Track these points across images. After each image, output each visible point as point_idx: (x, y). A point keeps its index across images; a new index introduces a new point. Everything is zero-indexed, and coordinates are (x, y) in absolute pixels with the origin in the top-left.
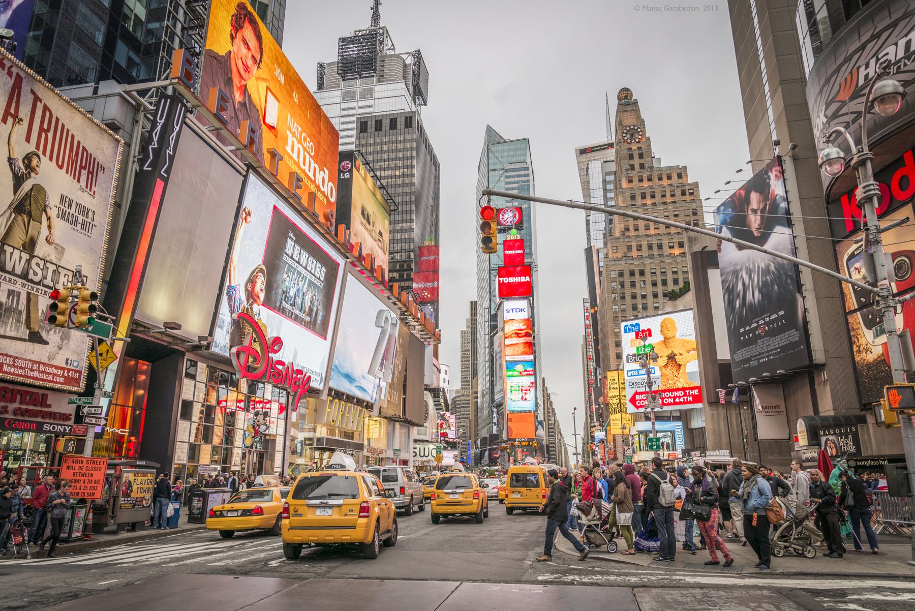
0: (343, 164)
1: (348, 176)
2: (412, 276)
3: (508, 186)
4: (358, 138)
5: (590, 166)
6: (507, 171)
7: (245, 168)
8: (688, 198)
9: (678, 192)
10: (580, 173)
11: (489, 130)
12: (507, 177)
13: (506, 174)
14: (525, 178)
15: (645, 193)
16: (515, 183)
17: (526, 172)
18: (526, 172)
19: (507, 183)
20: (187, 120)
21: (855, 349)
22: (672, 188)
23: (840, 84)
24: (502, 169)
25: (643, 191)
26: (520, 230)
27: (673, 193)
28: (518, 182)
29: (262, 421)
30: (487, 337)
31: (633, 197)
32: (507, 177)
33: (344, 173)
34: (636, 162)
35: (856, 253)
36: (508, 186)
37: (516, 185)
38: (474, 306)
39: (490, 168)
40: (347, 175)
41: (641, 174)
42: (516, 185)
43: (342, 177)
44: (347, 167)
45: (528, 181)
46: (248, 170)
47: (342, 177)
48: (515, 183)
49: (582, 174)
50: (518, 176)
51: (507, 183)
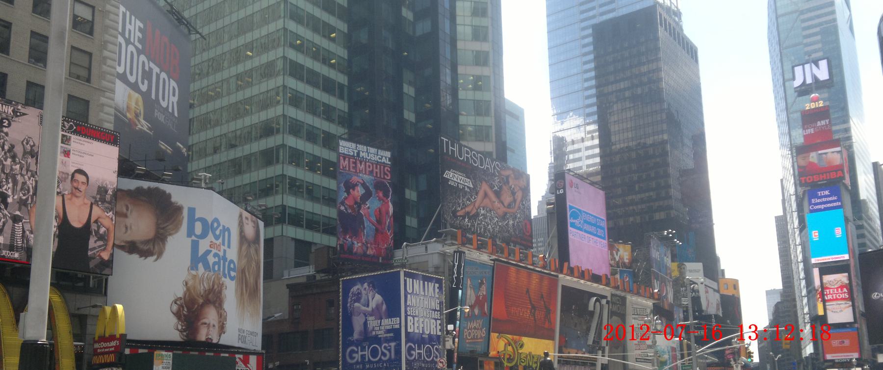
0: (558, 182)
6: (802, 12)
12: (803, 21)
13: (802, 17)
16: (815, 26)
17: (830, 9)
18: (830, 9)
19: (804, 29)
24: (795, 12)
28: (820, 24)
32: (803, 21)
33: (559, 190)
37: (818, 29)
39: (780, 12)
40: (561, 191)
42: (818, 29)
44: (561, 185)
45: (835, 20)
47: (558, 193)
48: (815, 26)
50: (819, 17)
51: (804, 29)
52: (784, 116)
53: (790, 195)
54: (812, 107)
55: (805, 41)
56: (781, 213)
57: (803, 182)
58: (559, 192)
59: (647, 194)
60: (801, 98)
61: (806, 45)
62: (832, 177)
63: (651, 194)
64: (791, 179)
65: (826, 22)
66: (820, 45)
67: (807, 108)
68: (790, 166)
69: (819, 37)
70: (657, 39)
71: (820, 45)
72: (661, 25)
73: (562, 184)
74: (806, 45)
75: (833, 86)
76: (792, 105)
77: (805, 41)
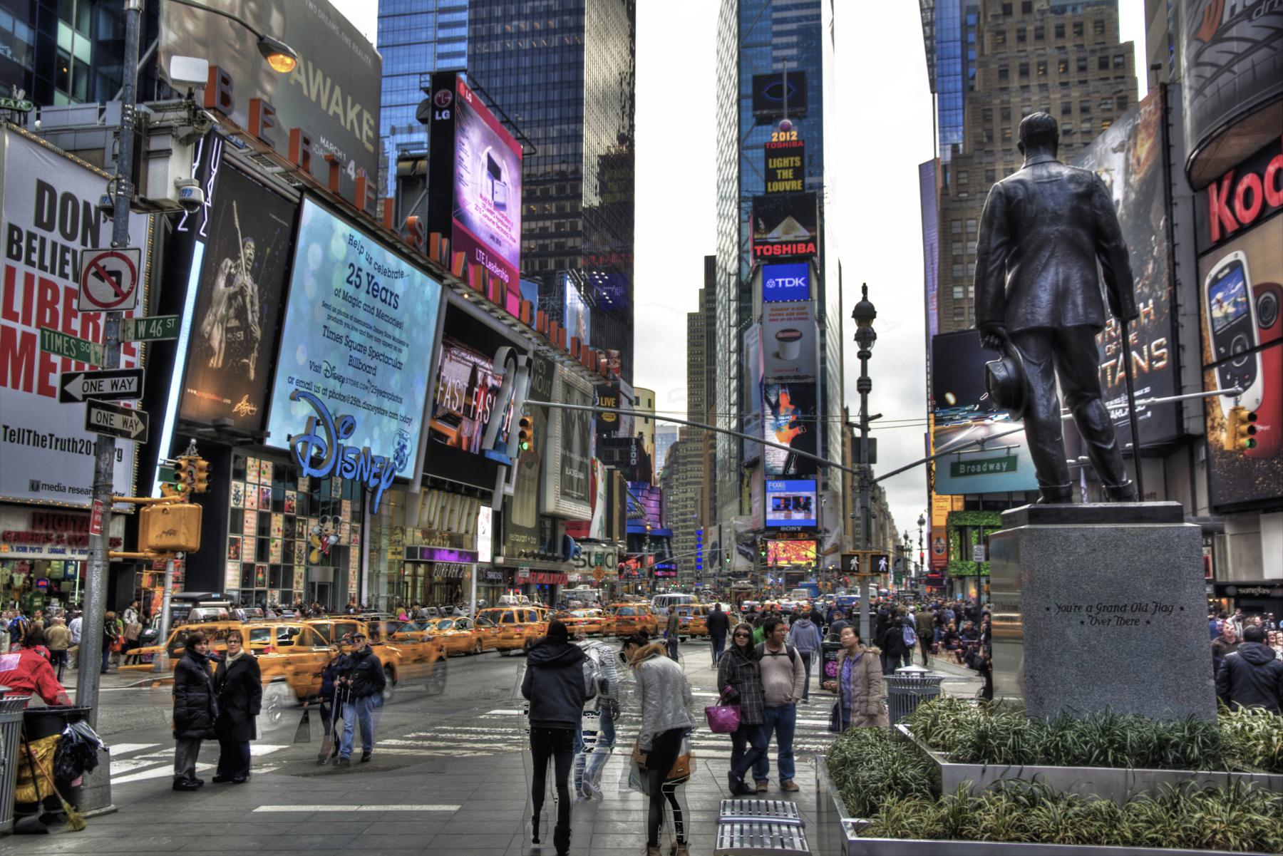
0: (439, 94)
1: (448, 117)
2: (580, 228)
3: (776, 28)
7: (298, 194)
8: (1110, 73)
9: (1093, 62)
15: (1027, 65)
20: (227, 156)
21: (1209, 423)
22: (1082, 55)
23: (1204, 12)
25: (1024, 60)
26: (800, 118)
27: (1082, 63)
28: (798, 19)
29: (331, 530)
30: (734, 331)
31: (1004, 74)
33: (441, 111)
35: (1220, 276)
36: (776, 28)
37: (794, 26)
38: (710, 263)
40: (446, 115)
41: (1021, 26)
43: (437, 118)
44: (446, 101)
46: (302, 195)
47: (437, 118)
52: (733, 152)
53: (730, 274)
54: (781, 139)
55: (775, 41)
57: (759, 253)
58: (440, 115)
59: (541, 224)
60: (760, 128)
61: (776, 47)
62: (799, 252)
63: (548, 223)
65: (807, 18)
66: (794, 52)
67: (775, 140)
68: (733, 229)
69: (794, 39)
71: (794, 52)
73: (450, 98)
74: (776, 47)
75: (805, 117)
76: (747, 136)
77: (775, 41)
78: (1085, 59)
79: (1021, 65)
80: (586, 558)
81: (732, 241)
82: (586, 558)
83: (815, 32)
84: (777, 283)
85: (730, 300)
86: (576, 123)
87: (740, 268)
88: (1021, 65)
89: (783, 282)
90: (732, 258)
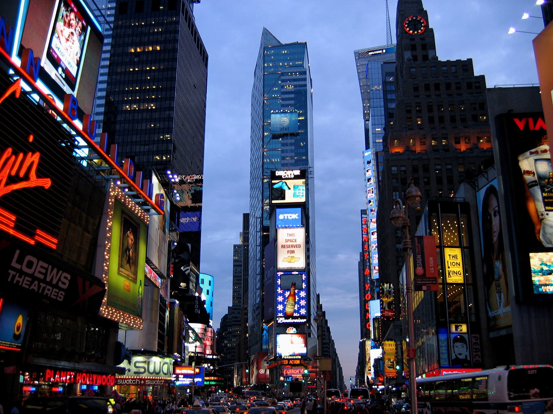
4: (116, 16)
5: (369, 67)
10: (359, 76)
11: (266, 33)
14: (302, 83)
15: (429, 85)
30: (259, 248)
34: (419, 53)
38: (246, 217)
45: (305, 85)
49: (361, 77)
53: (257, 218)
56: (239, 242)
60: (274, 140)
64: (259, 204)
69: (293, 96)
70: (177, 23)
72: (183, 12)
78: (459, 83)
79: (425, 85)
80: (146, 366)
81: (258, 199)
82: (146, 366)
83: (303, 93)
84: (284, 216)
85: (257, 232)
86: (169, 110)
87: (262, 214)
88: (425, 85)
89: (287, 216)
90: (258, 209)
